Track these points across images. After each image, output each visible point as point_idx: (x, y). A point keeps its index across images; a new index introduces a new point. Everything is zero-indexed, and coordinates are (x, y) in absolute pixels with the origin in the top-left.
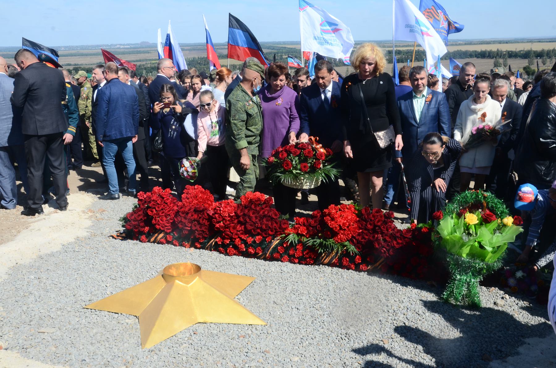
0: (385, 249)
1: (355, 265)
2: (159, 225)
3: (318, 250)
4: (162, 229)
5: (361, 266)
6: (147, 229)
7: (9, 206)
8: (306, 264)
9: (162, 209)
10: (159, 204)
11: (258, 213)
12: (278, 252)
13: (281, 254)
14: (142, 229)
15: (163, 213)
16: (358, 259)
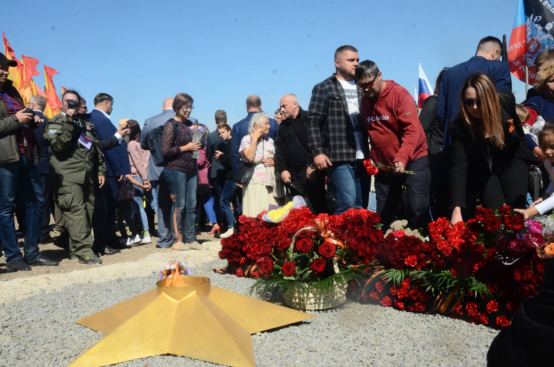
0: (532, 286)
1: (487, 315)
2: (250, 253)
3: (427, 286)
4: (253, 258)
5: (498, 318)
6: (243, 259)
7: (162, 245)
8: (415, 312)
9: (256, 234)
10: (252, 227)
11: (355, 235)
12: (376, 290)
13: (379, 293)
14: (236, 260)
15: (255, 238)
16: (492, 306)
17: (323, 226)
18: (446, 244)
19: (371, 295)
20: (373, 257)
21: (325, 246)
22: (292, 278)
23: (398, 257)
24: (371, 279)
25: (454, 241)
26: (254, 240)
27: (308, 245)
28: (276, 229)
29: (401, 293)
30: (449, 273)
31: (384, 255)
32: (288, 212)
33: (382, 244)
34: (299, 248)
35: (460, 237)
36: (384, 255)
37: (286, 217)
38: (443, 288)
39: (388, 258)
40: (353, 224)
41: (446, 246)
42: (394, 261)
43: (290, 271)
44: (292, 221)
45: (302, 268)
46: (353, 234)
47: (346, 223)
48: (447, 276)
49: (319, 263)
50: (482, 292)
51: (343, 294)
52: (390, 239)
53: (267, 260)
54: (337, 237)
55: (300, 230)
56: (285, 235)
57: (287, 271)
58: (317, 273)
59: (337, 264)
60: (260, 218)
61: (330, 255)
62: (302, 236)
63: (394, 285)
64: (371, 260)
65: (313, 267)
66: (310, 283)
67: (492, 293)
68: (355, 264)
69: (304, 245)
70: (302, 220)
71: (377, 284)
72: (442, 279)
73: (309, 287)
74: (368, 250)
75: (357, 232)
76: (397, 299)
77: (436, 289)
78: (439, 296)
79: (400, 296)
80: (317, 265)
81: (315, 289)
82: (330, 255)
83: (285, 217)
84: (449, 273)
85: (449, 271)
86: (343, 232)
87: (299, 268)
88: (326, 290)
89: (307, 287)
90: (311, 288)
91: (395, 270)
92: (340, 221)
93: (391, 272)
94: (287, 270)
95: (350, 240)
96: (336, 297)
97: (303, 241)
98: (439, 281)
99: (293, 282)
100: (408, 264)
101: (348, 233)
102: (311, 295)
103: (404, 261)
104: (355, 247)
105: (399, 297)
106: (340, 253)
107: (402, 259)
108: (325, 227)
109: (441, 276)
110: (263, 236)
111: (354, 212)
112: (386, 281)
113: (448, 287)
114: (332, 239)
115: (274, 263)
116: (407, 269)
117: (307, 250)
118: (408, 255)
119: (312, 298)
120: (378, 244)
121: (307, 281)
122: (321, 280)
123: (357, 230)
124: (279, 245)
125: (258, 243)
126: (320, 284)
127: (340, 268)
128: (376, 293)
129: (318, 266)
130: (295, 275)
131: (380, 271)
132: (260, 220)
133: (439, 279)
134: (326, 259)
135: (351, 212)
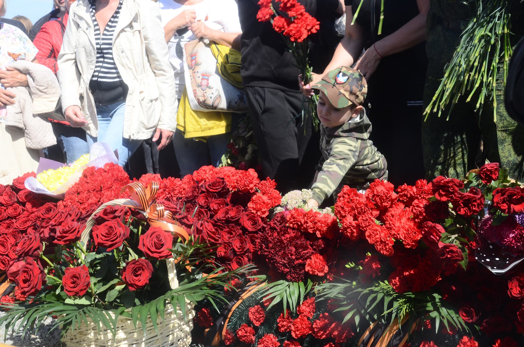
11: (212, 216)
12: (249, 323)
13: (256, 329)
15: (8, 227)
17: (148, 196)
18: (382, 232)
19: (240, 333)
20: (246, 259)
22: (84, 301)
23: (294, 257)
24: (240, 301)
25: (399, 227)
26: (7, 231)
27: (118, 234)
28: (53, 206)
29: (297, 327)
31: (266, 253)
32: (80, 175)
33: (262, 232)
34: (100, 241)
35: (409, 219)
36: (266, 253)
37: (76, 184)
38: (376, 317)
39: (274, 259)
40: (208, 194)
41: (382, 235)
42: (284, 265)
43: (78, 285)
44: (89, 191)
45: (105, 281)
46: (207, 214)
47: (196, 194)
48: (383, 292)
50: (448, 321)
51: (187, 331)
53: (31, 265)
54: (175, 217)
56: (71, 215)
57: (72, 285)
58: (134, 289)
59: (175, 271)
60: (19, 186)
61: (160, 253)
62: (106, 217)
63: (285, 312)
64: (240, 264)
65: (125, 278)
66: (120, 309)
67: (466, 323)
68: (209, 271)
69: (109, 234)
70: (109, 188)
71: (253, 310)
72: (375, 298)
73: (116, 317)
74: (236, 244)
75: (216, 212)
76: (290, 338)
77: (362, 318)
78: (367, 333)
79: (295, 332)
80: (135, 272)
81: (129, 322)
82: (160, 253)
83: (73, 183)
84: (387, 287)
85: (386, 282)
86: (188, 210)
87: (99, 282)
88: (151, 324)
89: (114, 318)
90: (122, 321)
91: (287, 283)
92: (184, 189)
93: (280, 287)
94: (73, 283)
95: (202, 225)
96: (171, 337)
97: (107, 225)
98: (368, 303)
99: (85, 309)
100: (312, 271)
101: (200, 213)
102: (121, 334)
103: (303, 265)
105: (293, 335)
106: (180, 250)
107: (300, 261)
108: (154, 200)
109: (372, 292)
110: (25, 222)
111: (211, 172)
112: (268, 306)
113: (386, 312)
114: (165, 222)
115: (46, 271)
116: (309, 280)
118: (313, 253)
119: (124, 340)
120: (256, 232)
121: (112, 306)
122: (142, 303)
123: (216, 207)
124: (58, 234)
125: (15, 237)
126: (140, 312)
127: (180, 279)
128: (249, 328)
129: (137, 276)
130: (89, 295)
131: (258, 284)
132: (20, 190)
133: (370, 298)
134: (153, 260)
135: (206, 173)
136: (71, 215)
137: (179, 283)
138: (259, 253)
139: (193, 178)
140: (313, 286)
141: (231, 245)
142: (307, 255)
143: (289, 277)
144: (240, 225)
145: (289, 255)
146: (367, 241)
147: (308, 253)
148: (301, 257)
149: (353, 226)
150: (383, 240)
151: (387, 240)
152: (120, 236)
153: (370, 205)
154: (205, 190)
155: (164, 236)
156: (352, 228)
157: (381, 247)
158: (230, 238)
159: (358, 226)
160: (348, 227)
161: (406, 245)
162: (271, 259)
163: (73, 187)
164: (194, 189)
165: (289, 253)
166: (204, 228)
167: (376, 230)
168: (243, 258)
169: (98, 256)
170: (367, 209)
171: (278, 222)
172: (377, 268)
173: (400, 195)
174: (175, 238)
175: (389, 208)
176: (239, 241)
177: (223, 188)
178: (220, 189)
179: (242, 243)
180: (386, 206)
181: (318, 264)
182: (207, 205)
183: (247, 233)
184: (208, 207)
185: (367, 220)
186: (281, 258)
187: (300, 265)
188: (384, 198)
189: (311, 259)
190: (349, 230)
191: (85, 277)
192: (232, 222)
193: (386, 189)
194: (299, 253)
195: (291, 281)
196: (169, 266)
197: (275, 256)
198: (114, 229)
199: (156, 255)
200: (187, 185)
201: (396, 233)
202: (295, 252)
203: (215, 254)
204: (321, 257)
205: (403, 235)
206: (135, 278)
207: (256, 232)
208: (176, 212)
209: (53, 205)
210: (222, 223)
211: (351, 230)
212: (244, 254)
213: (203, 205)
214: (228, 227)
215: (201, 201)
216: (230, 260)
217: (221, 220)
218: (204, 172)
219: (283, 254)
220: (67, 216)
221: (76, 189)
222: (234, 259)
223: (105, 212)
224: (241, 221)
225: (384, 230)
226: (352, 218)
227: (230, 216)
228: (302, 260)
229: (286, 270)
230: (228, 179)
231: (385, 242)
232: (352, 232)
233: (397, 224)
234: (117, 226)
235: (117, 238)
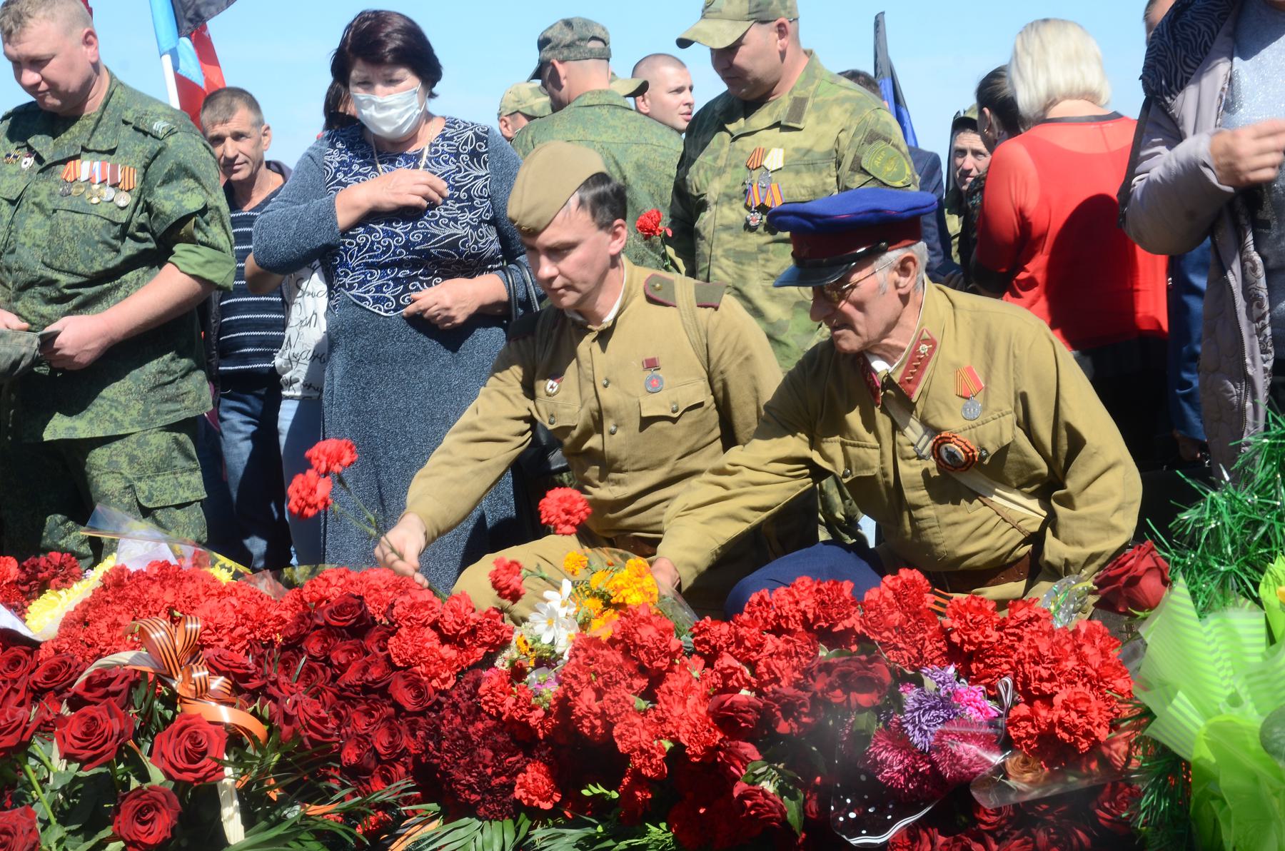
11: (334, 678)
21: (178, 736)
23: (489, 771)
28: (23, 654)
30: (663, 837)
33: (436, 712)
36: (436, 761)
37: (83, 603)
39: (450, 775)
40: (329, 632)
42: (469, 786)
46: (324, 672)
49: (150, 810)
52: (466, 696)
55: (90, 670)
56: (17, 691)
59: (236, 803)
61: (197, 771)
62: (88, 696)
69: (88, 734)
74: (381, 741)
75: (343, 668)
82: (197, 771)
83: (79, 602)
85: (663, 825)
93: (462, 832)
97: (84, 715)
101: (309, 671)
103: (511, 788)
104: (311, 727)
107: (504, 779)
114: (213, 704)
116: (523, 816)
117: (102, 754)
127: (249, 821)
129: (144, 823)
131: (424, 823)
135: (329, 585)
136: (17, 691)
137: (245, 831)
138: (423, 759)
139: (301, 597)
140: (532, 828)
141: (370, 739)
142: (518, 765)
143: (482, 811)
144: (389, 697)
145: (481, 766)
146: (616, 744)
147: (518, 762)
148: (505, 771)
149: (595, 714)
150: (645, 747)
151: (653, 748)
152: (112, 736)
153: (629, 668)
154: (322, 622)
155: (207, 733)
156: (592, 717)
157: (641, 761)
158: (370, 724)
159: (603, 715)
160: (585, 717)
161: (692, 756)
162: (446, 774)
163: (76, 609)
164: (301, 619)
165: (480, 762)
166: (301, 712)
167: (633, 725)
168: (395, 768)
169: (83, 774)
170: (622, 676)
171: (466, 692)
172: (645, 800)
173: (696, 641)
174: (235, 739)
175: (667, 671)
176: (386, 732)
177: (361, 618)
178: (353, 621)
179: (393, 735)
180: (659, 668)
181: (540, 784)
182: (325, 654)
183: (403, 714)
184: (327, 661)
185: (619, 701)
186: (463, 772)
187: (502, 785)
188: (655, 651)
189: (526, 772)
190: (586, 723)
191: (25, 832)
192: (375, 691)
193: (658, 631)
194: (501, 762)
195: (487, 818)
196: (222, 794)
197: (452, 768)
198: (100, 722)
199: (188, 776)
200: (290, 612)
201: (673, 731)
202: (492, 761)
203: (338, 760)
204: (543, 769)
205: (687, 736)
206: (140, 827)
207: (422, 713)
208: (246, 678)
209: (26, 651)
210: (356, 693)
211: (591, 722)
212: (397, 760)
213: (317, 655)
214: (366, 700)
215: (315, 647)
216: (369, 772)
217: (353, 686)
218: (326, 584)
219: (467, 764)
220: (8, 695)
221: (81, 614)
222: (377, 770)
223: (89, 684)
224: (390, 690)
225: (651, 723)
226: (593, 695)
227: (370, 679)
228: (507, 777)
229: (474, 797)
230: (376, 596)
231: (648, 751)
232: (593, 727)
233: (678, 710)
234: (106, 716)
235: (105, 742)
